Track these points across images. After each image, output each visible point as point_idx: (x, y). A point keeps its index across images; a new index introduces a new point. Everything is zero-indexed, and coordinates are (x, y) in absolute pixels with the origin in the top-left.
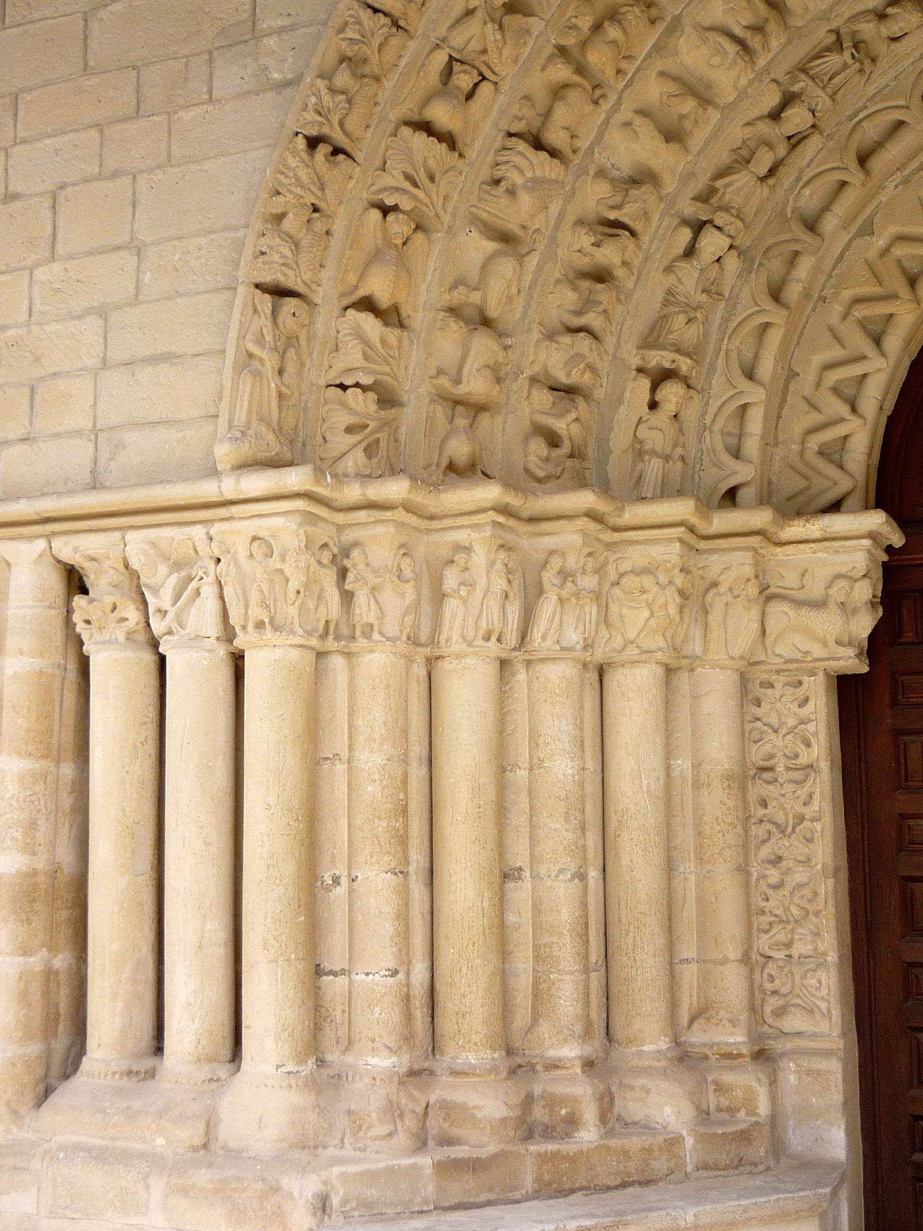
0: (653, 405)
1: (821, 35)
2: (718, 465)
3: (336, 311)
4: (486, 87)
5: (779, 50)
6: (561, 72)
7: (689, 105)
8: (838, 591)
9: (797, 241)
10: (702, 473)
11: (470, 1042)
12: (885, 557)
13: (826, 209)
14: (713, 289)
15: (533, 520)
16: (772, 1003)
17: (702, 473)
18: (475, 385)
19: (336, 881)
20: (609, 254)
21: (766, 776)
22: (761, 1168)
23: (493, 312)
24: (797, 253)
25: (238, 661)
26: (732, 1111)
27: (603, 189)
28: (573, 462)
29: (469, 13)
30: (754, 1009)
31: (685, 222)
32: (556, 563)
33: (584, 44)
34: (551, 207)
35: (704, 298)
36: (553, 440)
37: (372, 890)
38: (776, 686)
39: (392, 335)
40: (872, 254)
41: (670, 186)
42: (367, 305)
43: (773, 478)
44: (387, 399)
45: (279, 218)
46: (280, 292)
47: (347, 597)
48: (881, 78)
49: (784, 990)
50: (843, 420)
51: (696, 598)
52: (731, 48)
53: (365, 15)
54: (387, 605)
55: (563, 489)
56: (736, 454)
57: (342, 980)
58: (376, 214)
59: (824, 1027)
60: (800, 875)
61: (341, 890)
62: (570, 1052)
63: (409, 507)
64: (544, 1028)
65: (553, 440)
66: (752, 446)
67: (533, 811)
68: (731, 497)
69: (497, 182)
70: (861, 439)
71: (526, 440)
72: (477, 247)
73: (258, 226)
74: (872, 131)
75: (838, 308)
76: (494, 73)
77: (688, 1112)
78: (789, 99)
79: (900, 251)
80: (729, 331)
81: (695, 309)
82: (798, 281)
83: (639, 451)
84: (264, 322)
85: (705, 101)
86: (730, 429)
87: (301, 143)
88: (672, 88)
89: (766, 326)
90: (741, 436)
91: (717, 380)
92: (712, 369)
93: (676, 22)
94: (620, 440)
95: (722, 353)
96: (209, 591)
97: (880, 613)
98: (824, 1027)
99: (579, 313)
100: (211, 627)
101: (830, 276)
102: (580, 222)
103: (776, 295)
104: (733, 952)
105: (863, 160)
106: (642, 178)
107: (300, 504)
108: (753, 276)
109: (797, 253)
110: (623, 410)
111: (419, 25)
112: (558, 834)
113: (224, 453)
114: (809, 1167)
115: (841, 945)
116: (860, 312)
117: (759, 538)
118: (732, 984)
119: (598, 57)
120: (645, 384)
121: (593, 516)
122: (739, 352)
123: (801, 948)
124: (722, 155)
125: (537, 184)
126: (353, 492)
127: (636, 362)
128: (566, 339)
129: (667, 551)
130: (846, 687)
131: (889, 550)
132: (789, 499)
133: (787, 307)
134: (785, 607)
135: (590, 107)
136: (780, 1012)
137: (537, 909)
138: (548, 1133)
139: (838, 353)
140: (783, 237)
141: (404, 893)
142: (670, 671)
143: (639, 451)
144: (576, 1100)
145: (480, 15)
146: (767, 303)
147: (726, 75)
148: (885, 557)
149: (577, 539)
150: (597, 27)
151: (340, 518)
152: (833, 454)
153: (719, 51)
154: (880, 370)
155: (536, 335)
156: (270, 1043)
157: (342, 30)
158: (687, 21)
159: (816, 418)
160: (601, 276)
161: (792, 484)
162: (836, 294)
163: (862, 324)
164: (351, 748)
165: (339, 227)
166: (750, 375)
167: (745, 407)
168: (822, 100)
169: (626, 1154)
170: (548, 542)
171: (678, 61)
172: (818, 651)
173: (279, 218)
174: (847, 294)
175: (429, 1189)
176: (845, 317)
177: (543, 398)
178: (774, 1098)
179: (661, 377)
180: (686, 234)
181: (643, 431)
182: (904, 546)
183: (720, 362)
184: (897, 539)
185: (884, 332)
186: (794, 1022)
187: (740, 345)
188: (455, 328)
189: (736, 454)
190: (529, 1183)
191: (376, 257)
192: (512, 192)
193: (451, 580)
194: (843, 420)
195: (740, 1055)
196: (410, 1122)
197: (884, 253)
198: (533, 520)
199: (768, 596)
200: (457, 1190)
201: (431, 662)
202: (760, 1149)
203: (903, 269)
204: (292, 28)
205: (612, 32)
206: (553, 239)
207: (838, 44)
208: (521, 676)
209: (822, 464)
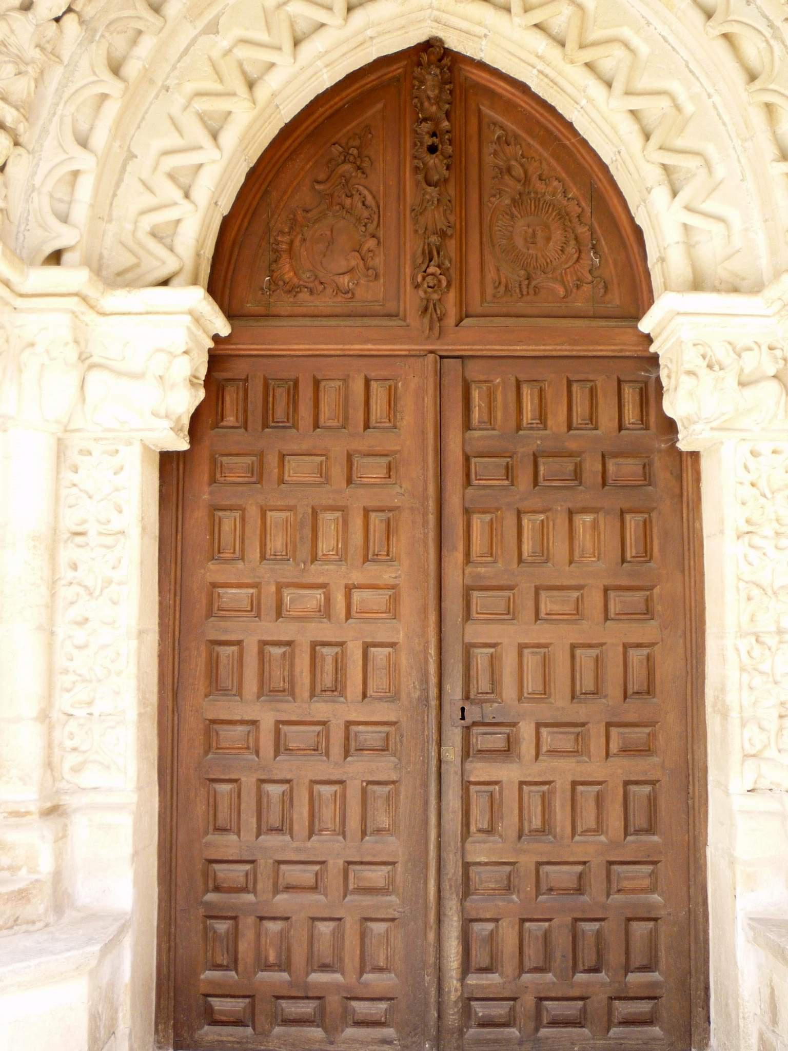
2: (44, 227)
9: (140, 18)
10: (26, 233)
12: (211, 345)
14: (49, 47)
16: (71, 760)
17: (26, 233)
21: (79, 539)
22: (39, 925)
24: (140, 32)
26: (13, 869)
35: (36, 54)
38: (93, 453)
43: (105, 253)
49: (83, 748)
50: (175, 204)
56: (64, 219)
66: (80, 213)
68: (56, 258)
70: (194, 227)
75: (179, 100)
79: (242, 53)
80: (66, 96)
81: (27, 64)
82: (138, 58)
86: (59, 195)
89: (104, 97)
92: (45, 131)
95: (56, 119)
97: (201, 394)
101: (174, 68)
103: (116, 69)
108: (94, 45)
109: (140, 32)
115: (143, 702)
116: (201, 105)
117: (76, 299)
122: (74, 121)
131: (216, 338)
132: (119, 274)
133: (124, 80)
136: (76, 770)
140: (126, 13)
146: (107, 75)
148: (211, 345)
154: (214, 161)
159: (148, 200)
162: (179, 84)
166: (84, 143)
167: (76, 174)
174: (189, 87)
176: (186, 108)
178: (59, 855)
182: (230, 335)
183: (53, 128)
184: (223, 328)
185: (221, 127)
189: (64, 219)
194: (175, 204)
195: (27, 813)
197: (228, 52)
199: (87, 362)
202: (39, 906)
203: (244, 73)
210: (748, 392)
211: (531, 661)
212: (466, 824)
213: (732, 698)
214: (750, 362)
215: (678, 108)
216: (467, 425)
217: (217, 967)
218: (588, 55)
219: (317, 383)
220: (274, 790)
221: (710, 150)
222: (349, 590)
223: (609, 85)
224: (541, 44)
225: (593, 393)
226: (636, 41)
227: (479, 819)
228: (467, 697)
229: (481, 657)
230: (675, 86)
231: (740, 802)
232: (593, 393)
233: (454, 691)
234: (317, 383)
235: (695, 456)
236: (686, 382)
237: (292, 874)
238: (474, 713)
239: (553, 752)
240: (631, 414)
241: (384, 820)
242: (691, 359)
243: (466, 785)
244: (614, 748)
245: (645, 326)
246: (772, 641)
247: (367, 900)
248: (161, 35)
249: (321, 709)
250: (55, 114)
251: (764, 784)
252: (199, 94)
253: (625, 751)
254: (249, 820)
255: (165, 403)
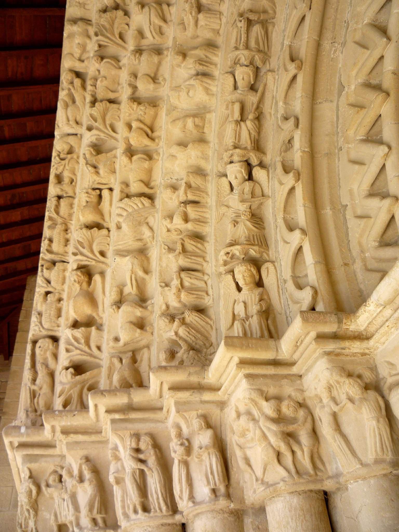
4: (105, 193)
76: (105, 184)
110: (222, 303)
135: (146, 164)
171: (180, 110)
248: (300, 126)
250: (277, 227)
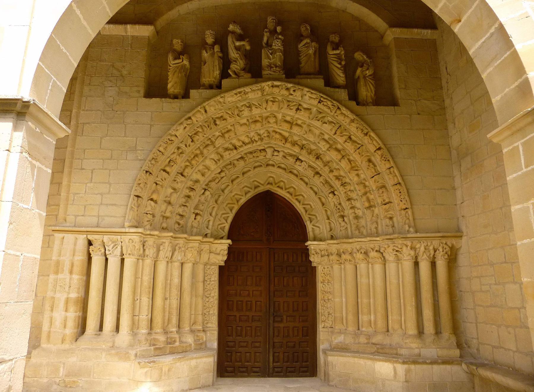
0: (195, 219)
1: (228, 162)
3: (147, 200)
5: (221, 163)
6: (188, 164)
7: (206, 170)
8: (222, 252)
11: (158, 329)
13: (225, 189)
15: (175, 238)
16: (206, 322)
18: (168, 214)
19: (137, 299)
20: (191, 194)
23: (172, 201)
25: (123, 260)
26: (199, 340)
27: (191, 183)
28: (183, 229)
29: (174, 153)
30: (203, 323)
31: (203, 189)
32: (178, 245)
33: (191, 159)
34: (182, 184)
36: (179, 224)
37: (145, 301)
39: (156, 205)
40: (232, 196)
41: (201, 183)
42: (152, 200)
44: (154, 216)
45: (139, 184)
46: (138, 196)
47: (144, 250)
48: (236, 169)
51: (200, 252)
52: (214, 162)
53: (158, 152)
54: (150, 252)
55: (180, 234)
56: (207, 228)
57: (137, 317)
58: (155, 184)
59: (214, 326)
60: (212, 300)
61: (138, 301)
62: (174, 330)
63: (157, 235)
64: (170, 326)
65: (179, 224)
66: (210, 227)
67: (170, 288)
68: (206, 235)
69: (175, 181)
70: (227, 226)
71: (175, 224)
72: (170, 190)
73: (135, 185)
74: (234, 177)
75: (225, 204)
77: (193, 340)
78: (222, 171)
79: (236, 196)
83: (192, 227)
84: (135, 202)
85: (209, 170)
87: (145, 172)
88: (204, 167)
90: (208, 225)
91: (205, 215)
93: (206, 158)
94: (189, 224)
96: (119, 247)
98: (214, 326)
99: (185, 203)
100: (119, 253)
102: (187, 188)
103: (216, 202)
104: (200, 313)
105: (232, 181)
106: (197, 181)
107: (140, 234)
111: (166, 154)
112: (175, 292)
113: (127, 224)
114: (211, 349)
116: (229, 206)
118: (200, 318)
119: (194, 162)
120: (194, 215)
121: (185, 238)
123: (211, 312)
124: (210, 178)
125: (182, 182)
126: (148, 232)
127: (193, 211)
128: (183, 207)
129: (196, 245)
130: (221, 267)
131: (229, 245)
134: (213, 254)
136: (207, 323)
137: (170, 305)
138: (170, 343)
139: (225, 212)
141: (149, 302)
142: (194, 264)
143: (192, 227)
144: (176, 338)
145: (176, 154)
146: (215, 203)
147: (213, 166)
149: (182, 242)
150: (194, 157)
151: (145, 236)
152: (223, 229)
153: (212, 162)
155: (178, 206)
156: (126, 328)
157: (154, 154)
158: (208, 158)
159: (220, 222)
160: (189, 197)
161: (215, 233)
163: (229, 207)
164: (142, 276)
165: (148, 186)
167: (209, 221)
168: (227, 172)
169: (183, 347)
170: (177, 242)
172: (218, 262)
173: (139, 184)
174: (227, 202)
175: (153, 353)
177: (178, 217)
179: (197, 214)
180: (203, 191)
181: (193, 224)
184: (231, 244)
186: (209, 325)
187: (210, 210)
188: (166, 204)
189: (207, 228)
190: (168, 352)
191: (154, 192)
192: (177, 183)
193: (161, 248)
196: (149, 341)
197: (234, 196)
198: (175, 238)
200: (157, 352)
201: (155, 262)
204: (143, 150)
205: (197, 159)
206: (182, 190)
207: (231, 164)
208: (170, 264)
209: (221, 230)
210: (323, 258)
211: (286, 305)
212: (274, 335)
213: (320, 311)
214: (323, 253)
215: (311, 207)
216: (274, 261)
217: (228, 362)
218: (297, 197)
219: (247, 253)
220: (239, 328)
221: (317, 215)
222: (253, 291)
223: (300, 202)
224: (288, 195)
225: (297, 255)
226: (304, 195)
227: (276, 334)
228: (274, 310)
229: (277, 303)
230: (311, 203)
231: (321, 329)
232: (297, 255)
233: (272, 310)
234: (247, 253)
235: (315, 267)
236: (313, 256)
237: (242, 344)
238: (275, 314)
239: (289, 321)
240: (304, 259)
241: (259, 334)
242: (313, 252)
243: (274, 327)
244: (301, 320)
245: (306, 244)
246: (327, 301)
247: (256, 349)
249: (248, 313)
251: (325, 326)
252: (229, 204)
253: (303, 321)
254: (234, 334)
255: (221, 259)
